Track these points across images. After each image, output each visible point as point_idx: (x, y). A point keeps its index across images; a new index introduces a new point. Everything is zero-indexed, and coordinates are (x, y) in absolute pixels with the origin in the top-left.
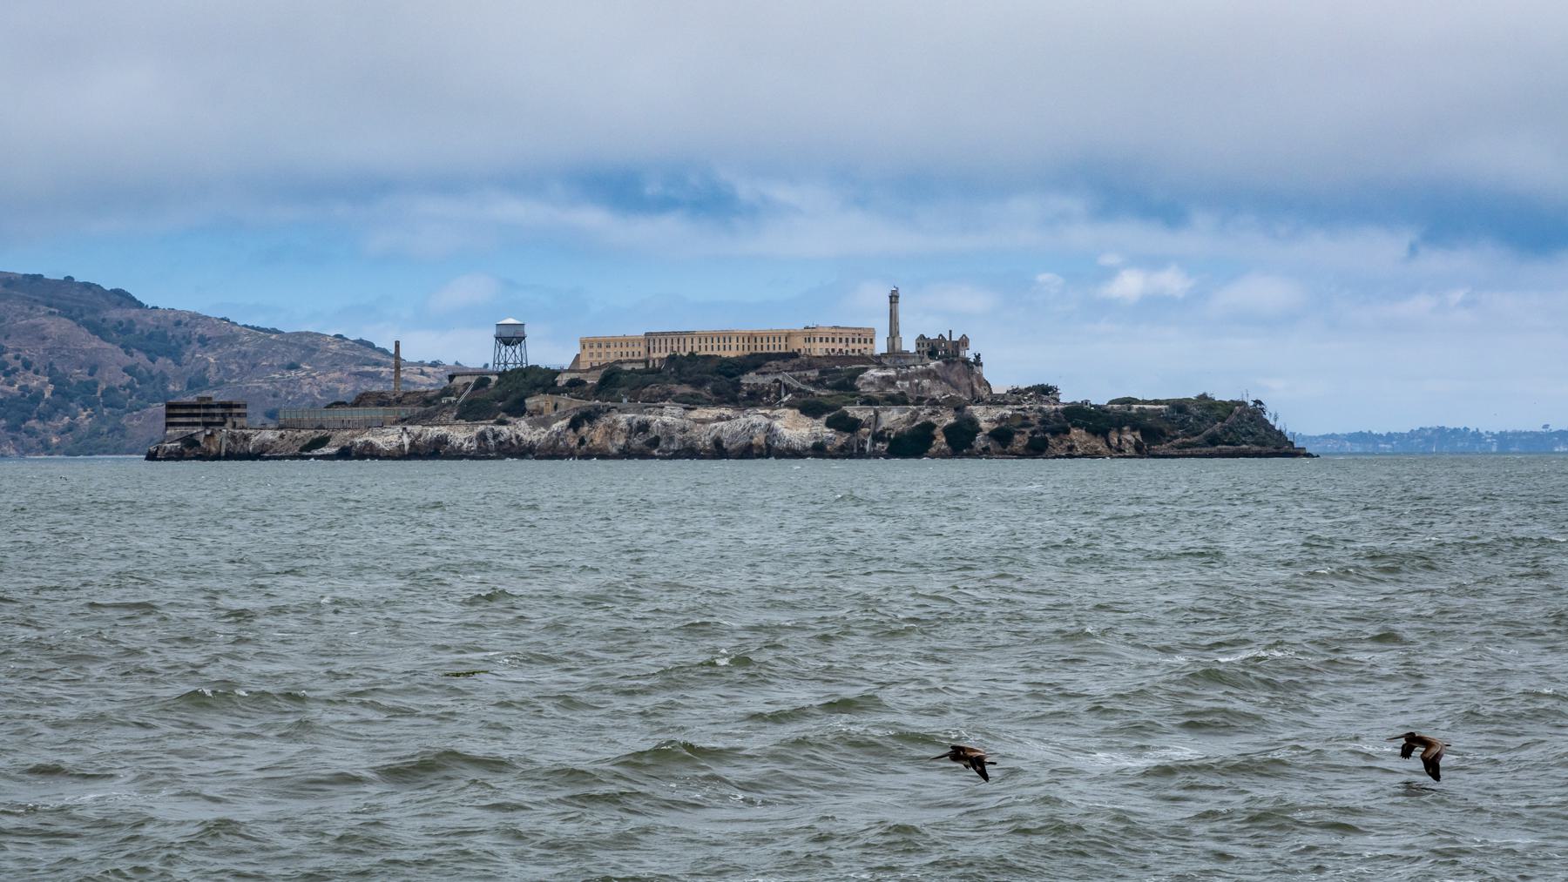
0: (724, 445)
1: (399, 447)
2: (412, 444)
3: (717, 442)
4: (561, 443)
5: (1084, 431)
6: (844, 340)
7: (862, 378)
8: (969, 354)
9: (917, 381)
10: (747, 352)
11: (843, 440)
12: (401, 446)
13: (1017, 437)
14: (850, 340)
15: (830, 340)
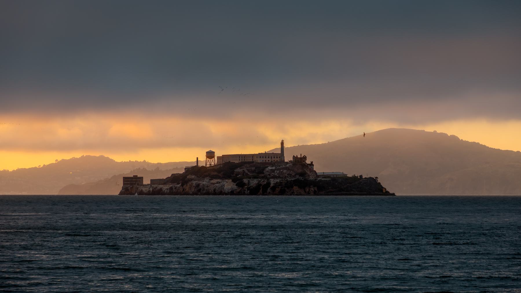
0: (216, 191)
1: (149, 191)
2: (153, 190)
3: (215, 190)
4: (179, 190)
5: (297, 187)
6: (270, 157)
7: (266, 170)
8: (308, 162)
9: (282, 170)
10: (241, 161)
11: (240, 189)
12: (149, 191)
13: (277, 189)
14: (273, 157)
15: (264, 157)
